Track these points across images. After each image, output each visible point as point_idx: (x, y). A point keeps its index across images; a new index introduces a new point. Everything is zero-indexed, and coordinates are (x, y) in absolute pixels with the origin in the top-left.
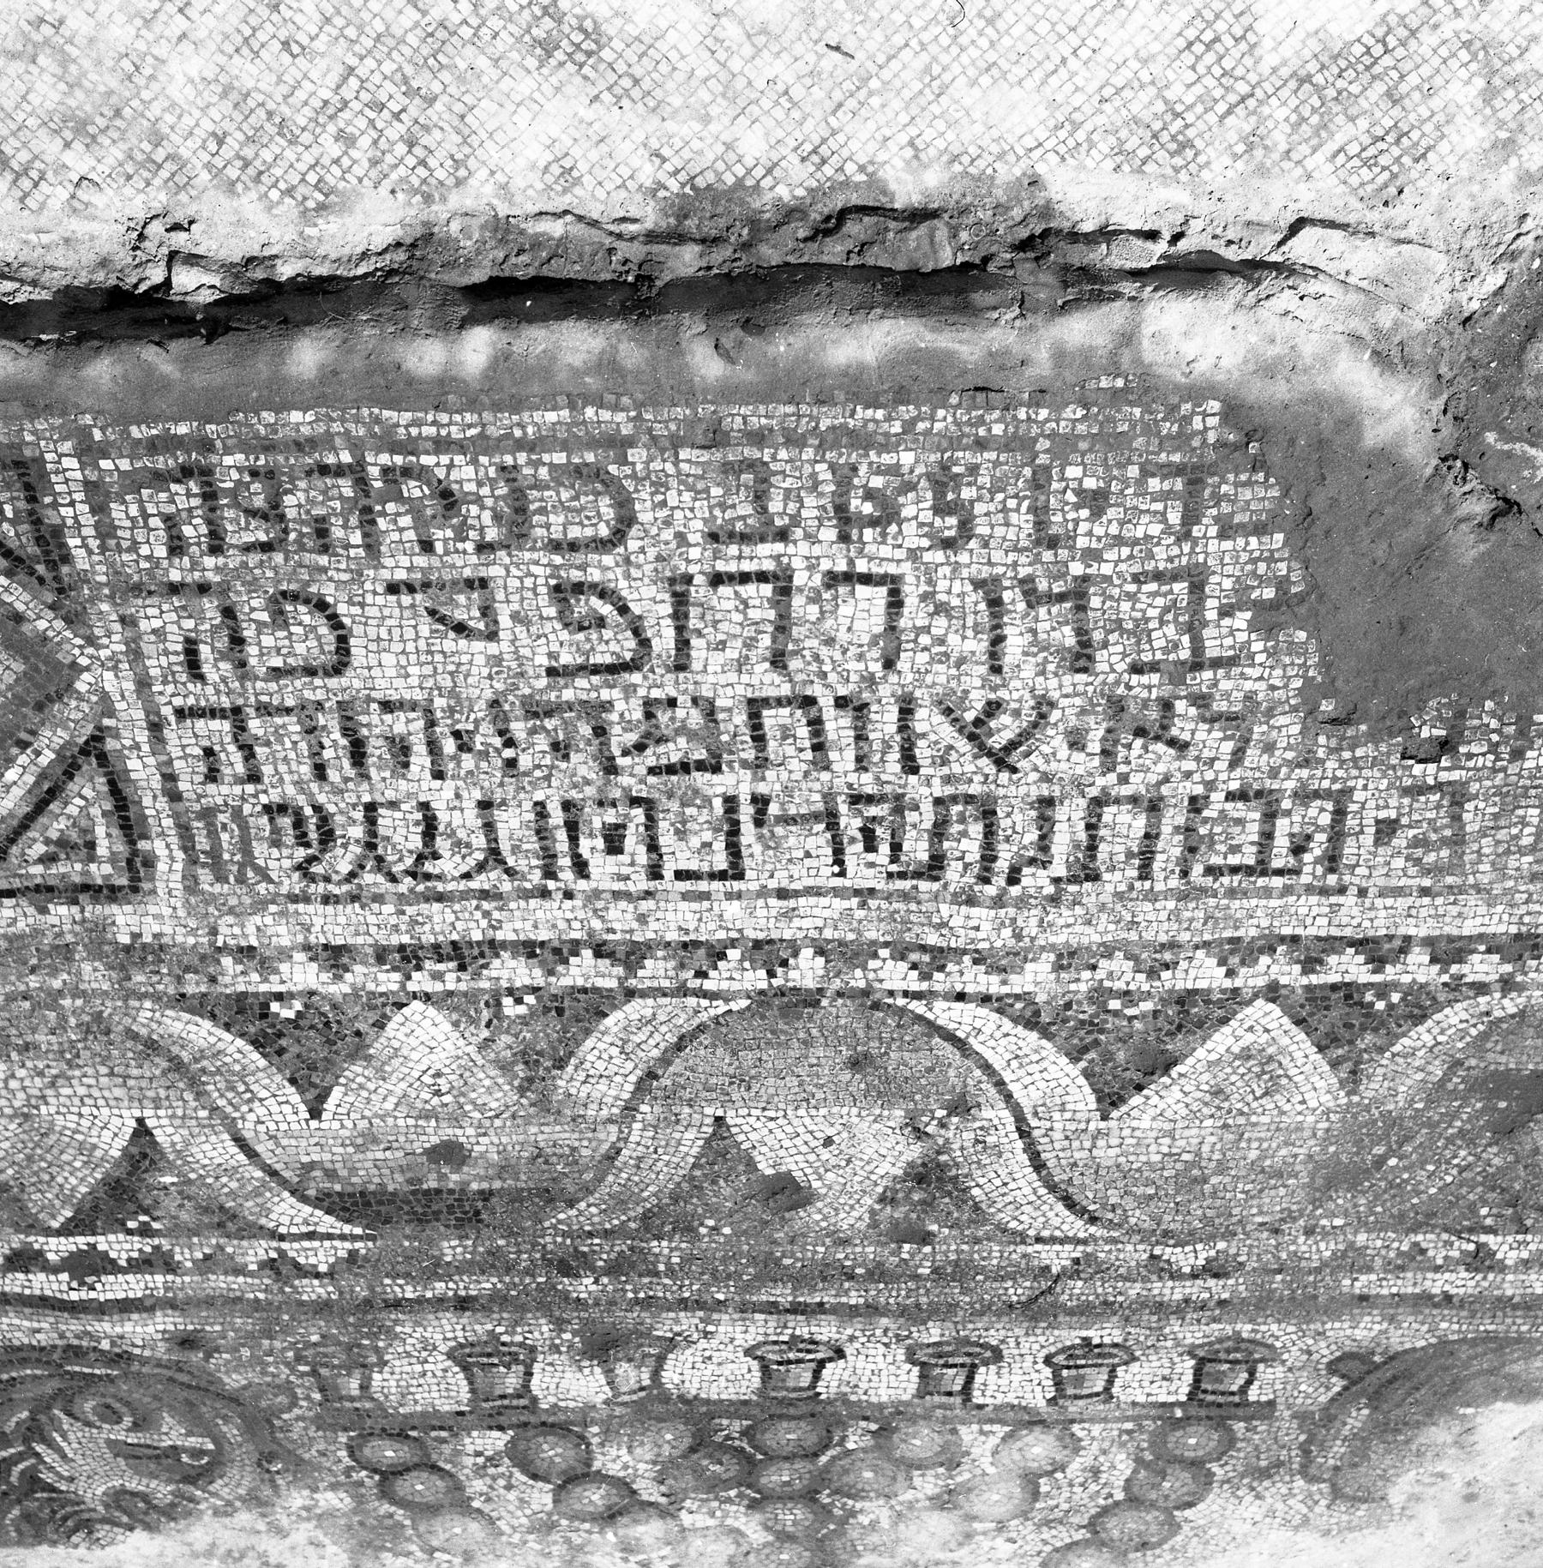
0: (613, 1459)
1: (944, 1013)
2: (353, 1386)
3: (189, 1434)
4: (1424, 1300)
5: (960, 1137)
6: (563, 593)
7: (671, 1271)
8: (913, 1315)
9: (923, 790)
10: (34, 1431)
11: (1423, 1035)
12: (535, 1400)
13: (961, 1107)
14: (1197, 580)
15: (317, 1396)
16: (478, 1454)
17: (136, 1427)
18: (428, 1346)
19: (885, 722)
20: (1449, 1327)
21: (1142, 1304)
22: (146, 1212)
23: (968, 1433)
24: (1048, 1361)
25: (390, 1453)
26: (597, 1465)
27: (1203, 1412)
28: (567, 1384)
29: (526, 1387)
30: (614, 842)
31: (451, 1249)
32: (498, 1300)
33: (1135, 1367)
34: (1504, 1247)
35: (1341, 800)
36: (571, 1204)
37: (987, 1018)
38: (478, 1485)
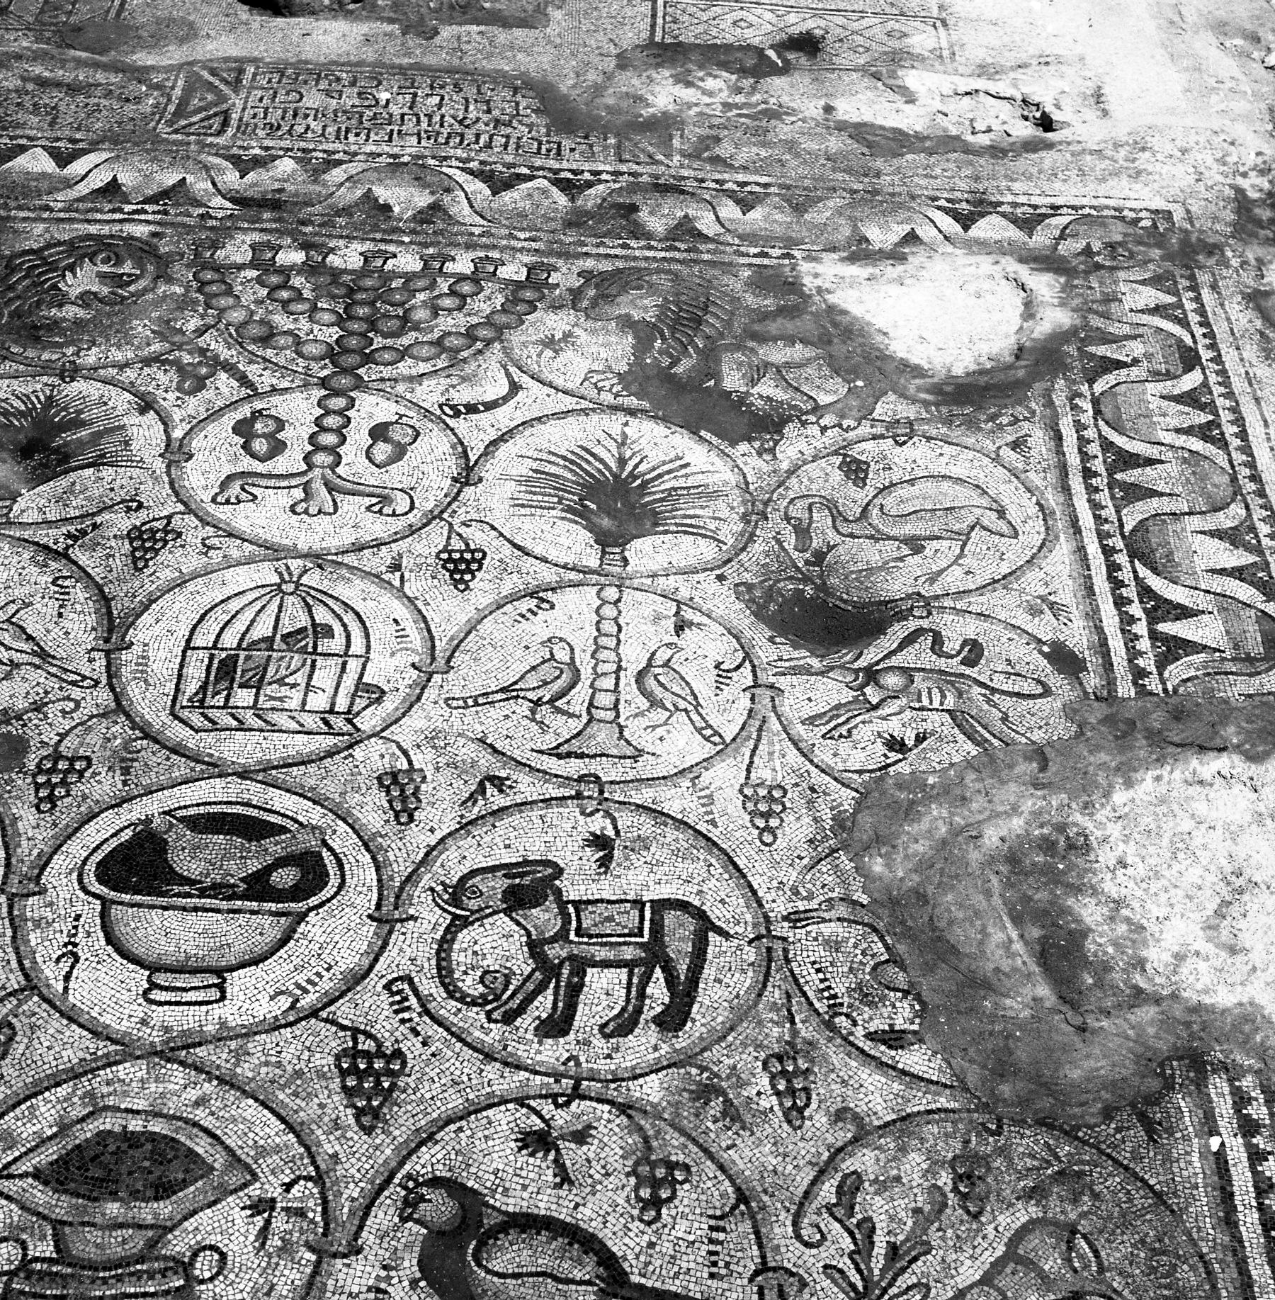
0: (297, 281)
1: (444, 170)
4: (607, 256)
5: (447, 199)
6: (359, 94)
8: (426, 246)
9: (445, 131)
10: (71, 268)
11: (592, 191)
13: (448, 190)
14: (517, 104)
18: (244, 242)
19: (437, 119)
20: (620, 264)
21: (506, 247)
25: (209, 276)
28: (292, 257)
30: (357, 135)
31: (266, 216)
32: (277, 230)
34: (633, 243)
35: (559, 144)
37: (458, 172)
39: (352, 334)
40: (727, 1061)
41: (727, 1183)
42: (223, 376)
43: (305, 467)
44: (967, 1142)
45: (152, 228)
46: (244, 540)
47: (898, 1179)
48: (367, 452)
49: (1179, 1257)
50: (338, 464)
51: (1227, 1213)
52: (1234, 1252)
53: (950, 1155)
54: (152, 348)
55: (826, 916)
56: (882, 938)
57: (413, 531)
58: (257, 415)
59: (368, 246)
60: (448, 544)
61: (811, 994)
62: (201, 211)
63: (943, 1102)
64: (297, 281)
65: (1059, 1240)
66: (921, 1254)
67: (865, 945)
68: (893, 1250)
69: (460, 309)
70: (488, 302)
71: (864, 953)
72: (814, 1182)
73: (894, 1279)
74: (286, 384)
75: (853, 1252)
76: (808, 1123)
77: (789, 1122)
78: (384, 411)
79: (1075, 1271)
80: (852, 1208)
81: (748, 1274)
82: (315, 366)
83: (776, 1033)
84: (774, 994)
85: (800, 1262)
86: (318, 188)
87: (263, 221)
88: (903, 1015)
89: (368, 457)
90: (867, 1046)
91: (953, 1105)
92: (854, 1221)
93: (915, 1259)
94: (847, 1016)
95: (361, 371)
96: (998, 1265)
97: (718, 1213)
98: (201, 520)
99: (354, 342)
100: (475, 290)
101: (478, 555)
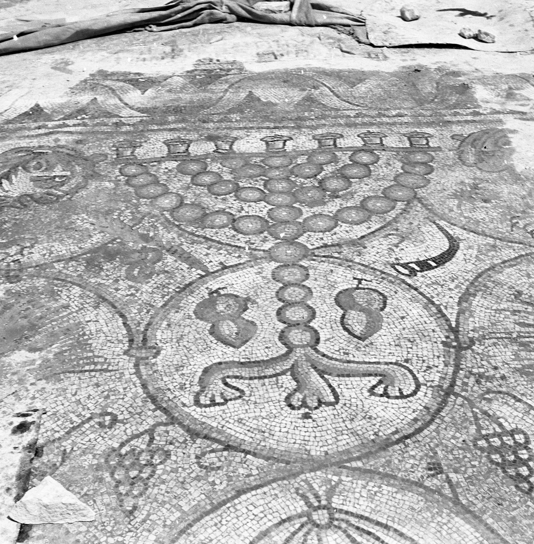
0: (215, 167)
2: (129, 153)
3: (64, 170)
4: (467, 122)
5: (316, 93)
7: (237, 121)
12: (189, 153)
15: (115, 156)
16: (166, 168)
17: (46, 169)
22: (85, 114)
23: (338, 154)
24: (358, 136)
25: (132, 170)
26: (208, 169)
27: (417, 150)
29: (187, 150)
31: (171, 118)
32: (184, 129)
33: (388, 138)
36: (208, 108)
38: (165, 177)
39: (279, 206)
42: (170, 259)
43: (285, 350)
45: (76, 137)
46: (247, 452)
48: (342, 323)
50: (318, 341)
54: (95, 239)
57: (433, 415)
58: (214, 294)
59: (265, 133)
60: (479, 428)
62: (115, 120)
64: (215, 167)
69: (369, 175)
70: (388, 169)
74: (233, 261)
78: (343, 279)
82: (256, 240)
86: (208, 95)
87: (169, 123)
89: (346, 329)
95: (302, 240)
98: (188, 430)
99: (283, 214)
100: (372, 158)
101: (520, 438)
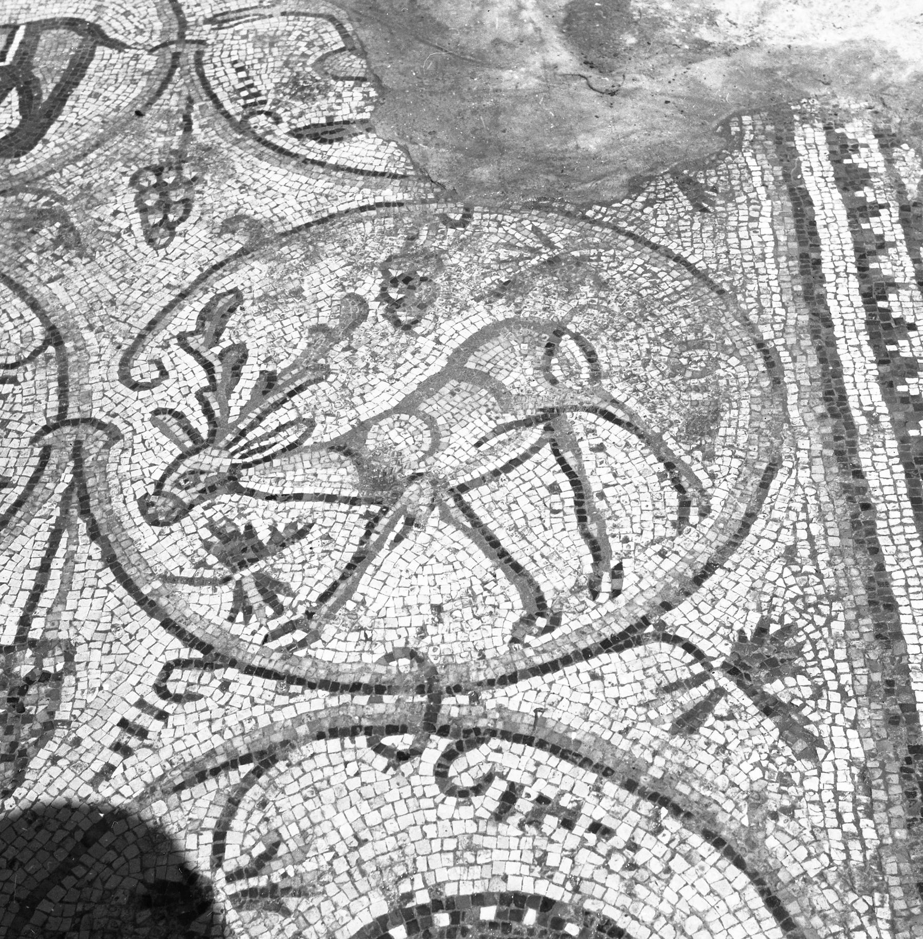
40: (79, 181)
41: (37, 321)
44: (412, 238)
47: (297, 293)
49: (724, 348)
51: (808, 287)
52: (815, 334)
53: (383, 257)
55: (267, 12)
56: (340, 27)
61: (222, 95)
63: (390, 194)
65: (534, 344)
66: (310, 382)
67: (313, 36)
68: (269, 381)
71: (310, 45)
72: (166, 310)
73: (260, 418)
75: (206, 389)
76: (178, 240)
77: (150, 241)
79: (554, 381)
80: (218, 334)
81: (33, 431)
83: (159, 141)
84: (171, 101)
85: (118, 410)
88: (350, 103)
90: (290, 144)
91: (400, 197)
92: (217, 350)
93: (300, 389)
94: (268, 114)
96: (429, 387)
97: (12, 360)
